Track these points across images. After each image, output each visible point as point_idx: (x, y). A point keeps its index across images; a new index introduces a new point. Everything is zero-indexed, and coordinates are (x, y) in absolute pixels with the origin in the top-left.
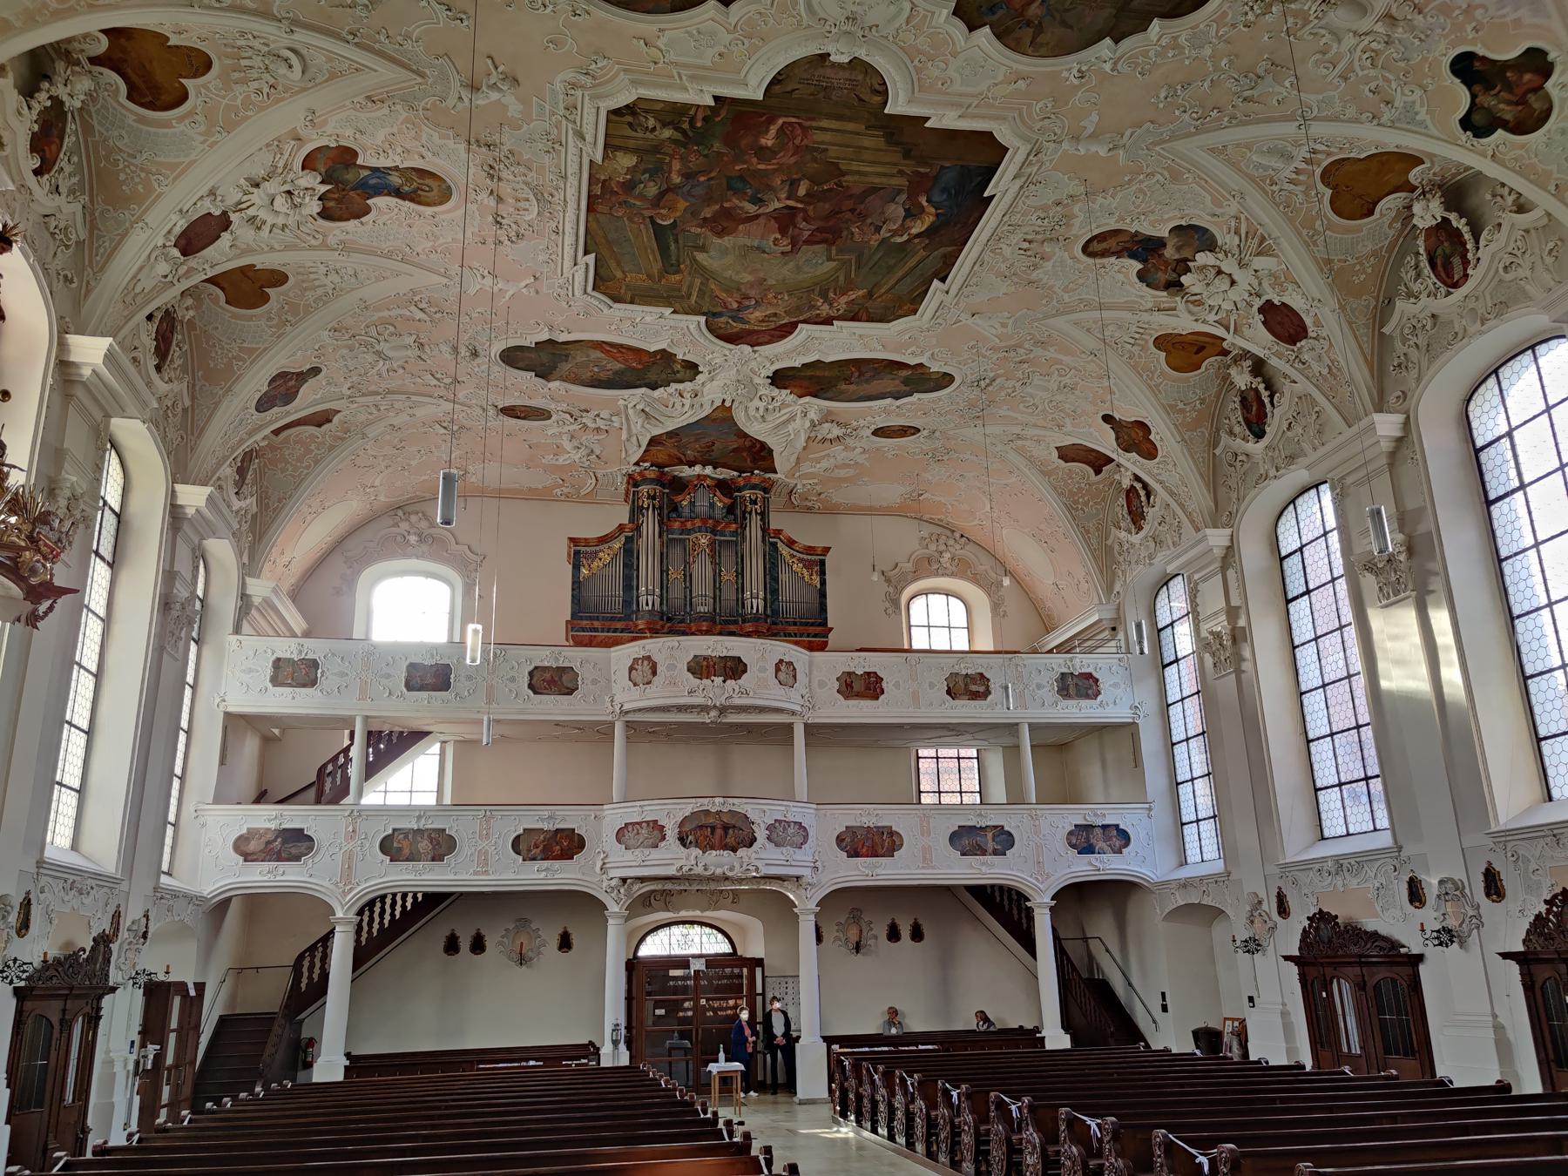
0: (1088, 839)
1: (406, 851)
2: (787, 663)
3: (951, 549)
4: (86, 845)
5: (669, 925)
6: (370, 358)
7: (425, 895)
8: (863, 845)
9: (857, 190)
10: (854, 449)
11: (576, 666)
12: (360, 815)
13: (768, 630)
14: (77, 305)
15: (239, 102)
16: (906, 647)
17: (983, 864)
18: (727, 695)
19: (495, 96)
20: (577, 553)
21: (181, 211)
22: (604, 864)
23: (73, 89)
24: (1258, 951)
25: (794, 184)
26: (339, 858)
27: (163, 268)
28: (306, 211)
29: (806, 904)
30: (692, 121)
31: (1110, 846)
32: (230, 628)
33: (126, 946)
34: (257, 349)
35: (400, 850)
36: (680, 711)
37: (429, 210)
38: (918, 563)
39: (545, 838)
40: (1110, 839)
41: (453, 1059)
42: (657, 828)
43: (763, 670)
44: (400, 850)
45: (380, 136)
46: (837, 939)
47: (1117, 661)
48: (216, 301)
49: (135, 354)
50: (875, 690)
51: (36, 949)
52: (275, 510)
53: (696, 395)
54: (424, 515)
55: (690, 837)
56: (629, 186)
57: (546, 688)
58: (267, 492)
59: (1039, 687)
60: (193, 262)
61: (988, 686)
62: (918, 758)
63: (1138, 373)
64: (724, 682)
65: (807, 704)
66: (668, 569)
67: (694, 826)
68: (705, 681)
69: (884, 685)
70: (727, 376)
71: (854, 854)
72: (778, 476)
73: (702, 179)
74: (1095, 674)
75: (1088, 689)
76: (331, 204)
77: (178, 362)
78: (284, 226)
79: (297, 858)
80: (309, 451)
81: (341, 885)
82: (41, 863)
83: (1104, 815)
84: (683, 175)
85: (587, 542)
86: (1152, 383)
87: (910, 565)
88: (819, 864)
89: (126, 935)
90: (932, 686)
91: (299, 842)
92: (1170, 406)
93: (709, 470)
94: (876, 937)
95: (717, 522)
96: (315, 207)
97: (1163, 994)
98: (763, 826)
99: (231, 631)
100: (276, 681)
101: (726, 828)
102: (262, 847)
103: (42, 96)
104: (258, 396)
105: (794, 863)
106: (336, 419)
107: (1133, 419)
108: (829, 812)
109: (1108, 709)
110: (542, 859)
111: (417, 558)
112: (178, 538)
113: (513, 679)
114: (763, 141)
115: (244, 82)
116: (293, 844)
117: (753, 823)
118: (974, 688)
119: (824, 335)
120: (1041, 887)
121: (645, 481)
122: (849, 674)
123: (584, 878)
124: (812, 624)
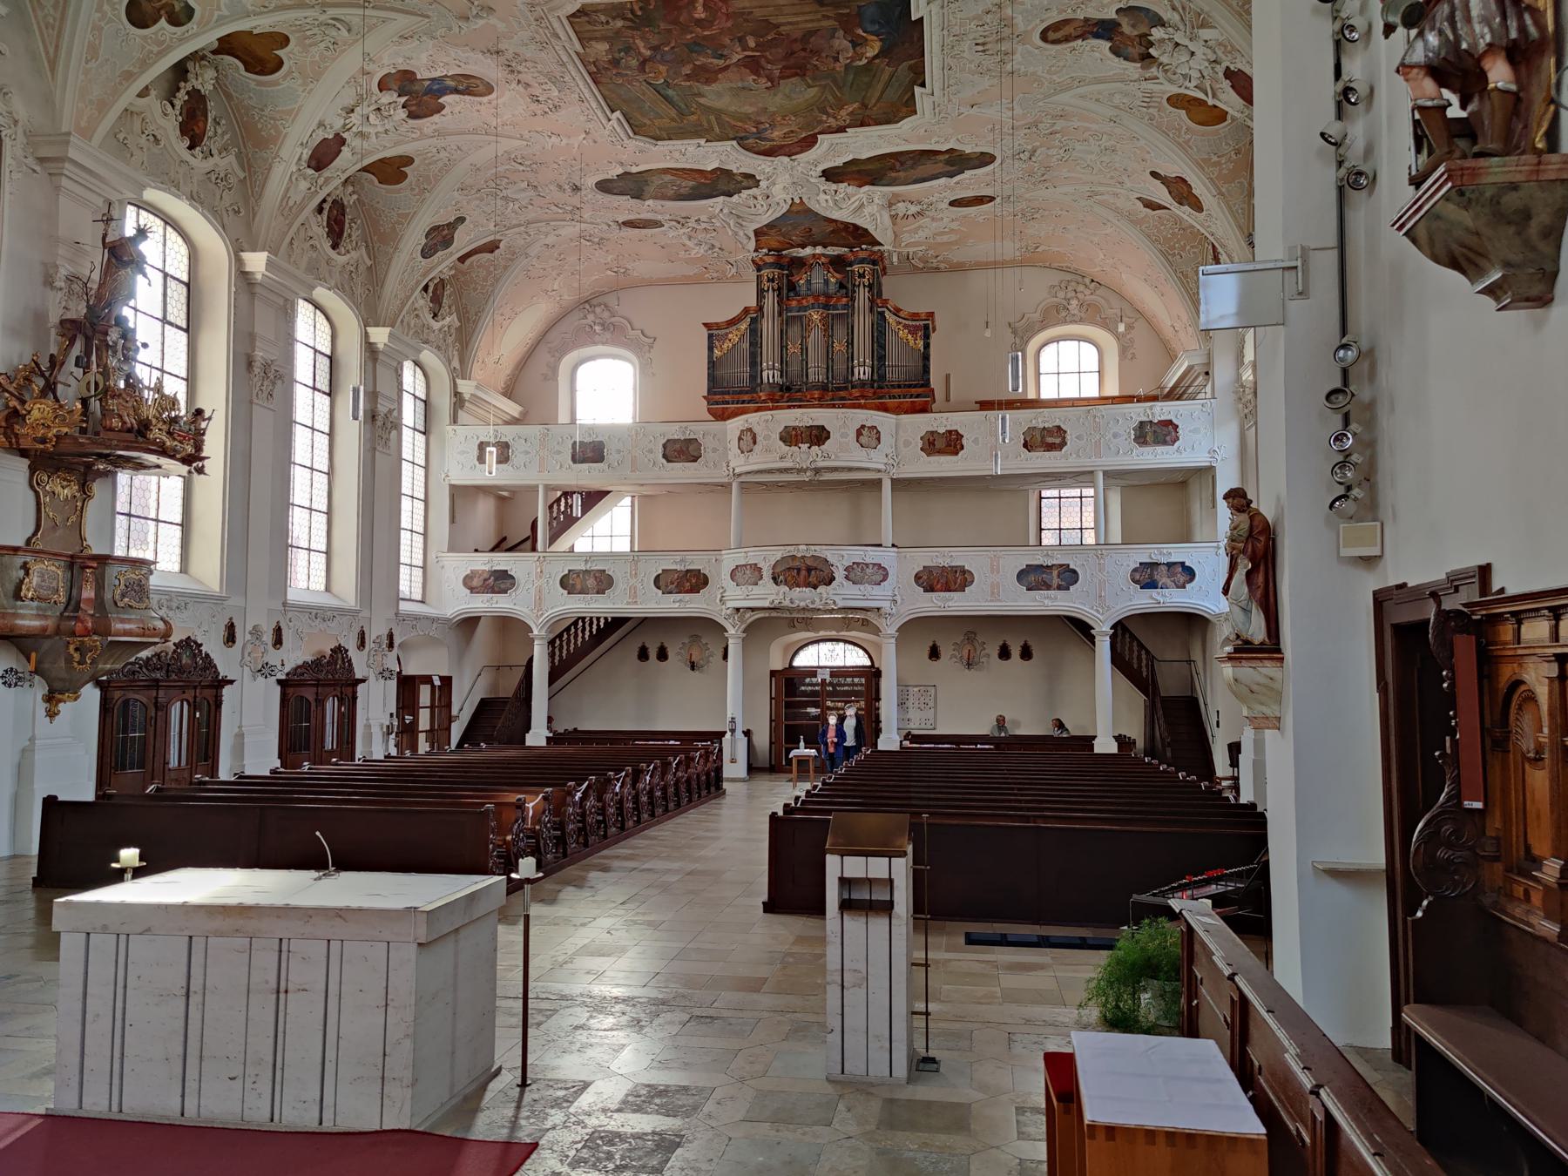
0: (1151, 576)
1: (578, 587)
4: (335, 587)
5: (817, 642)
6: (499, 202)
9: (798, 34)
10: (942, 219)
11: (699, 437)
13: (874, 393)
14: (249, 225)
15: (317, 58)
16: (1031, 395)
19: (481, 22)
20: (710, 336)
21: (302, 144)
23: (204, 80)
25: (741, 40)
26: (533, 591)
27: (304, 185)
28: (396, 118)
30: (632, 11)
31: (1174, 581)
32: (447, 421)
37: (485, 99)
38: (1046, 311)
40: (1174, 575)
41: (593, 736)
42: (756, 569)
43: (844, 435)
45: (424, 57)
46: (953, 656)
48: (371, 182)
49: (312, 242)
50: (955, 446)
51: (294, 656)
52: (474, 321)
53: (768, 197)
54: (606, 306)
56: (615, 63)
59: (1115, 436)
60: (327, 173)
61: (1064, 438)
62: (1041, 498)
63: (1164, 132)
65: (891, 461)
66: (787, 345)
69: (964, 441)
70: (783, 180)
71: (930, 589)
73: (666, 49)
74: (1175, 421)
76: (414, 108)
78: (386, 131)
80: (489, 273)
82: (285, 604)
83: (1170, 553)
84: (650, 49)
85: (718, 326)
86: (1181, 140)
87: (1037, 315)
88: (898, 598)
89: (373, 645)
92: (1203, 160)
93: (819, 250)
94: (988, 656)
95: (828, 296)
96: (402, 114)
98: (841, 569)
99: (448, 422)
101: (809, 570)
103: (182, 96)
106: (502, 245)
107: (1174, 175)
108: (908, 555)
111: (603, 344)
112: (378, 366)
113: (651, 451)
114: (697, 16)
115: (315, 44)
116: (500, 582)
118: (1050, 440)
119: (842, 140)
121: (767, 265)
122: (932, 433)
124: (915, 386)
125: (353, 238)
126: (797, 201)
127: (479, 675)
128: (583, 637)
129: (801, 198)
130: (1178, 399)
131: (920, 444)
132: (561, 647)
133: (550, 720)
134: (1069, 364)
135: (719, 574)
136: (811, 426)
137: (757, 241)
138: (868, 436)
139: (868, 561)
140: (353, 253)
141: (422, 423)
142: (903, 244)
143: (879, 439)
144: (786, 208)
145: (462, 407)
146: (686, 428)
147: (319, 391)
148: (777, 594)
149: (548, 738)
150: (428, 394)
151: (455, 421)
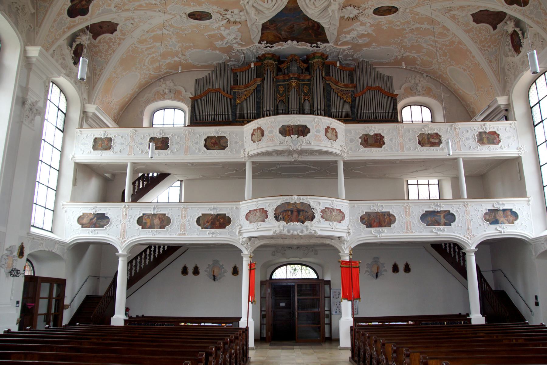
0: (495, 217)
1: (149, 224)
7: (168, 247)
17: (440, 230)
22: (240, 230)
26: (120, 227)
31: (507, 220)
35: (146, 223)
36: (278, 155)
39: (212, 218)
42: (264, 213)
44: (146, 223)
46: (367, 271)
47: (509, 125)
50: (380, 142)
52: (99, 75)
55: (280, 216)
57: (212, 147)
58: (95, 67)
61: (440, 139)
64: (298, 138)
67: (282, 210)
68: (287, 137)
69: (385, 140)
71: (369, 225)
72: (330, 44)
75: (493, 139)
79: (103, 227)
88: (351, 231)
90: (410, 140)
91: (103, 219)
97: (536, 297)
98: (319, 211)
100: (94, 148)
101: (299, 211)
102: (88, 221)
104: (67, 8)
105: (336, 230)
109: (504, 150)
111: (169, 99)
117: (313, 209)
118: (433, 140)
120: (470, 241)
122: (366, 135)
127: (86, 281)
128: (150, 259)
131: (360, 141)
132: (136, 266)
133: (127, 310)
135: (238, 216)
136: (298, 125)
137: (262, 34)
139: (335, 207)
142: (339, 43)
143: (337, 136)
146: (219, 130)
148: (279, 226)
149: (125, 321)
150: (67, 111)
151: (81, 126)
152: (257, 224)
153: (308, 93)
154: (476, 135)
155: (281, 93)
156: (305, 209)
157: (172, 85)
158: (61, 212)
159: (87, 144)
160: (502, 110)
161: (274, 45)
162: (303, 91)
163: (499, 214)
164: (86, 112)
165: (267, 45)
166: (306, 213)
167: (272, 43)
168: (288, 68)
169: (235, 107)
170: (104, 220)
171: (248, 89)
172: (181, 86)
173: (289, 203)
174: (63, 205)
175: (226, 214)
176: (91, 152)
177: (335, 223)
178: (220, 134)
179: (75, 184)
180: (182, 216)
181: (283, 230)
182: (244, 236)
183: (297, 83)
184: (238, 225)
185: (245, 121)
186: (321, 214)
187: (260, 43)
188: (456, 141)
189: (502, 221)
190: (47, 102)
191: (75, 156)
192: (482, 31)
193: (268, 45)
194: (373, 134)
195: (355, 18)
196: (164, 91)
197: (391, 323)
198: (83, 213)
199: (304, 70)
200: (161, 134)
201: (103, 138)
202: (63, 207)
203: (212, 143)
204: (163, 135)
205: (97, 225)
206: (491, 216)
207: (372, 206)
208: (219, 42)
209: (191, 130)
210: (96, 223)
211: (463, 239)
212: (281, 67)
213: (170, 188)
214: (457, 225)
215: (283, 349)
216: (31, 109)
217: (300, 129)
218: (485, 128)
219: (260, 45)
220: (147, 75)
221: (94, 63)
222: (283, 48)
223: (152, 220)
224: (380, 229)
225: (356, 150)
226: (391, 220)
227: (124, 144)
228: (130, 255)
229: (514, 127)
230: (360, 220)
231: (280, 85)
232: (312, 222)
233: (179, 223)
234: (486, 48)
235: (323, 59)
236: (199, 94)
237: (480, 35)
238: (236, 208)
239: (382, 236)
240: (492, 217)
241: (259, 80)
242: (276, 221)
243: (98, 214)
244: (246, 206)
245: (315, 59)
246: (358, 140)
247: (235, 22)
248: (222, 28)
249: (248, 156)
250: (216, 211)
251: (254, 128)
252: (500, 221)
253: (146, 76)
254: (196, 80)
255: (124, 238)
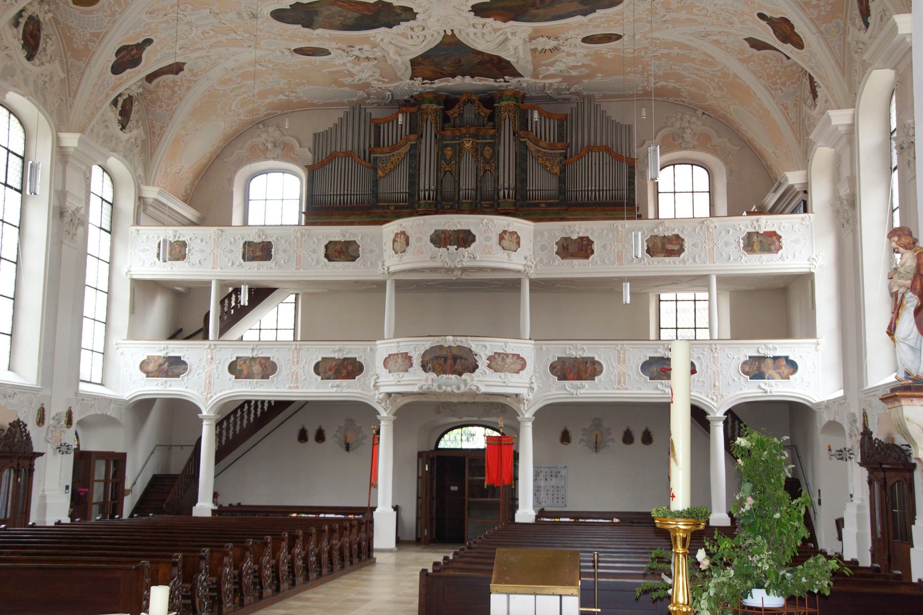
0: (759, 368)
1: (245, 372)
2: (510, 233)
3: (693, 126)
7: (277, 402)
8: (570, 372)
12: (215, 348)
18: (459, 260)
22: (376, 383)
24: (851, 458)
26: (203, 376)
29: (527, 414)
31: (779, 373)
33: (52, 428)
34: (102, 32)
35: (241, 371)
39: (336, 364)
42: (407, 358)
44: (241, 371)
46: (581, 440)
50: (586, 250)
52: (159, 135)
53: (423, 29)
55: (429, 365)
57: (336, 257)
58: (152, 123)
61: (682, 245)
64: (457, 249)
67: (432, 356)
69: (595, 247)
71: (563, 377)
74: (779, 233)
77: (50, 50)
79: (178, 376)
81: (205, 394)
88: (535, 386)
89: (52, 422)
98: (484, 358)
99: (132, 224)
101: (455, 358)
102: (157, 368)
104: (110, 65)
105: (509, 384)
106: (186, 67)
109: (786, 262)
110: (334, 379)
111: (274, 159)
112: (68, 168)
117: (476, 355)
118: (669, 247)
122: (566, 239)
123: (363, 392)
125: (48, 52)
126: (449, 33)
127: (152, 453)
128: (248, 420)
129: (452, 30)
130: (781, 213)
131: (555, 248)
132: (228, 429)
133: (215, 495)
134: (684, 184)
137: (413, 70)
138: (509, 240)
139: (509, 351)
140: (47, 65)
141: (108, 223)
143: (518, 243)
144: (439, 39)
145: (145, 210)
147: (11, 187)
149: (213, 511)
151: (137, 222)
152: (399, 375)
153: (491, 158)
154: (743, 239)
155: (448, 158)
156: (465, 356)
157: (277, 134)
158: (116, 355)
159: (149, 251)
160: (798, 193)
161: (436, 81)
162: (482, 155)
163: (766, 363)
164: (142, 197)
165: (424, 82)
166: (466, 361)
167: (432, 79)
168: (461, 115)
169: (376, 183)
170: (179, 366)
171: (396, 152)
172: (293, 137)
173: (441, 347)
174: (117, 344)
175: (356, 358)
176: (155, 263)
177: (509, 375)
178: (347, 237)
179: (133, 311)
180: (293, 359)
181: (433, 385)
182: (381, 391)
183: (473, 142)
184: (373, 375)
185: (391, 206)
186: (488, 362)
187: (412, 79)
188: (707, 248)
189: (769, 375)
190: (89, 195)
191: (131, 269)
192: (768, 61)
193: (426, 81)
194: (576, 238)
195: (556, 49)
196: (264, 144)
197: (587, 521)
198: (148, 357)
199: (486, 119)
200: (260, 236)
201: (172, 241)
202: (117, 346)
203: (335, 251)
204: (263, 239)
205: (170, 374)
206: (753, 366)
207: (568, 349)
208: (347, 79)
209: (304, 231)
210: (167, 371)
211: (704, 400)
212: (449, 114)
213: (281, 305)
214: (696, 379)
215: (436, 552)
216: (71, 220)
217: (461, 235)
218: (759, 226)
219: (412, 82)
220: (235, 122)
221: (150, 117)
222: (449, 84)
223: (250, 366)
224: (578, 383)
225: (550, 262)
226: (595, 369)
227: (204, 251)
228: (219, 417)
229: (808, 224)
230: (550, 370)
231: (446, 146)
232: (473, 375)
233: (288, 371)
234: (778, 87)
235: (516, 99)
236: (320, 160)
237: (765, 66)
238: (371, 349)
239: (580, 394)
240: (755, 368)
241: (413, 137)
242: (424, 372)
243: (170, 357)
244: (385, 347)
245: (503, 101)
246: (552, 247)
247: (368, 58)
248: (349, 65)
249: (389, 273)
250: (342, 355)
251: (396, 232)
252: (767, 376)
253: (234, 124)
254: (315, 135)
255: (210, 392)
